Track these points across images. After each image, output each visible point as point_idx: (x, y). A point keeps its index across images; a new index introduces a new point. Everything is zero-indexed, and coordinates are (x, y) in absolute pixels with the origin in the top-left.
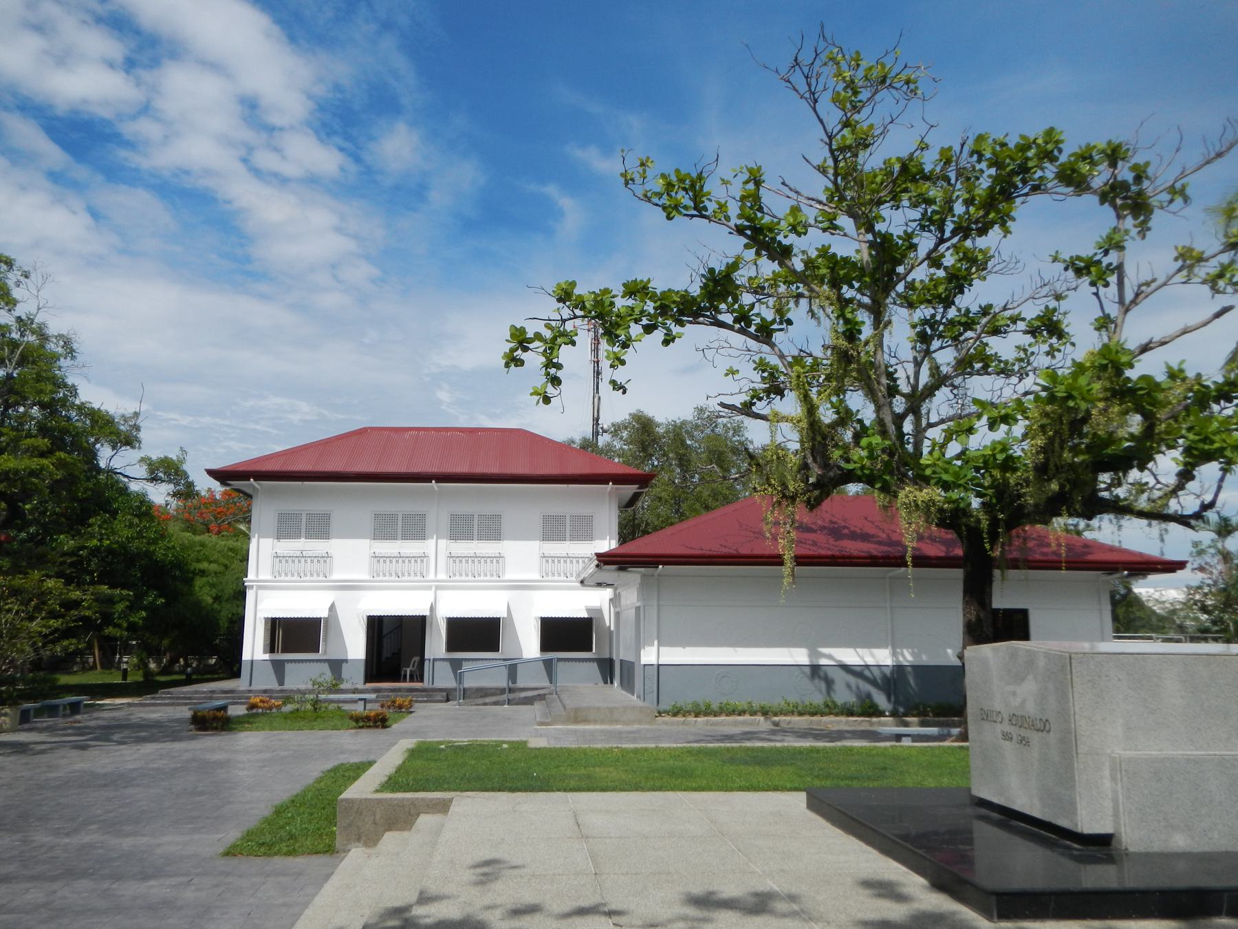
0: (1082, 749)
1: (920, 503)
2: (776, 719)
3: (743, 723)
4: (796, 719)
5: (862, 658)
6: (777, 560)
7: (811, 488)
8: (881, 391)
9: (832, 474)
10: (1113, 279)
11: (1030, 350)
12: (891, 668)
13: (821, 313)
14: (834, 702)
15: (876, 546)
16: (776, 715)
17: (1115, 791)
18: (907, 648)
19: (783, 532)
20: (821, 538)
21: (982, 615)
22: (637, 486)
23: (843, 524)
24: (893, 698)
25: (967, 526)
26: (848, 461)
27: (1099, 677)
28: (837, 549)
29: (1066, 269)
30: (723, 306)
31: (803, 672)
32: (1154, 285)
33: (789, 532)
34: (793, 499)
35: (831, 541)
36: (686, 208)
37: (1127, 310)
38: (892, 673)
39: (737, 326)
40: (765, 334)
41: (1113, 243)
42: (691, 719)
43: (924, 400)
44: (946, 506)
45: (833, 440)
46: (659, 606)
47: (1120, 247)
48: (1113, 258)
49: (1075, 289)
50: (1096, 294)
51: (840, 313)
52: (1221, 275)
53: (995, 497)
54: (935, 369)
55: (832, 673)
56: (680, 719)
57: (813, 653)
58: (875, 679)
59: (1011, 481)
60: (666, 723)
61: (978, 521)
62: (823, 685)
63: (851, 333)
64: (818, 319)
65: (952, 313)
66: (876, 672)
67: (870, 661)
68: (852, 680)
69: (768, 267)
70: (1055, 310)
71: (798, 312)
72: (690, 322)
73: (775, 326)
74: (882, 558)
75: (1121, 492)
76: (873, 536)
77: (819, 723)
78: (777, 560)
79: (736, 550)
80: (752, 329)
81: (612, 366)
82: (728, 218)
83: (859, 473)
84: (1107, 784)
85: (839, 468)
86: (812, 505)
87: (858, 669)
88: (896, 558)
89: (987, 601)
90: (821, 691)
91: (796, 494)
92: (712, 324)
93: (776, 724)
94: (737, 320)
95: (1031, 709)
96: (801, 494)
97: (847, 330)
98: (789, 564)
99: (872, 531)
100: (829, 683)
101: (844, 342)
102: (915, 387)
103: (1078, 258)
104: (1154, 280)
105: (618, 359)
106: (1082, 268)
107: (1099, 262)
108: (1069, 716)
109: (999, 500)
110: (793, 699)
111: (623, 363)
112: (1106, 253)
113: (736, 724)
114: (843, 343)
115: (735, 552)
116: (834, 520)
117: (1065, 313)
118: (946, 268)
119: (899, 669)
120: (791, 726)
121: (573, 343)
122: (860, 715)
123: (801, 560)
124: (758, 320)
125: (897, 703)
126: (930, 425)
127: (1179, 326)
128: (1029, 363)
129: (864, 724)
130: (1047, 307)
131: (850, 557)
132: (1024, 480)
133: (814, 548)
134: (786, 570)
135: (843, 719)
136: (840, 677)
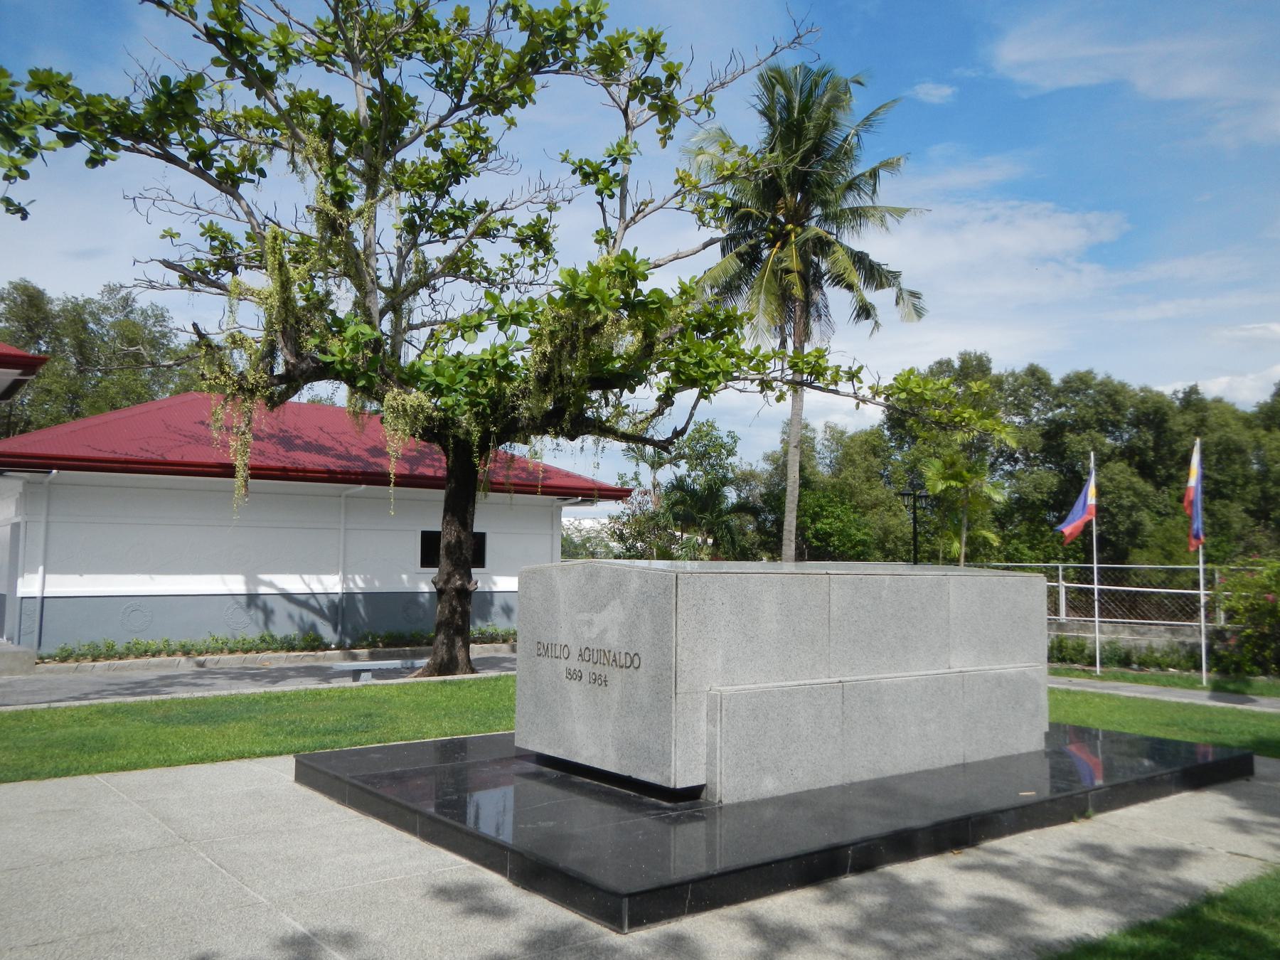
0: (682, 687)
1: (408, 407)
2: (201, 658)
3: (158, 666)
4: (226, 657)
5: (308, 586)
6: (227, 471)
7: (276, 381)
8: (369, 274)
9: (304, 366)
10: (617, 191)
12: (340, 595)
14: (272, 636)
15: (334, 460)
16: (200, 654)
17: (711, 736)
18: (359, 574)
19: (237, 433)
20: (269, 447)
21: (463, 537)
22: (19, 371)
23: (295, 433)
24: (339, 628)
25: (455, 437)
26: (324, 352)
27: (704, 600)
28: (287, 461)
29: (574, 172)
30: (175, 136)
31: (237, 603)
32: (651, 207)
33: (244, 433)
34: (252, 392)
35: (282, 451)
37: (627, 227)
38: (341, 600)
39: (193, 165)
40: (228, 182)
41: (620, 155)
42: (87, 664)
43: (407, 297)
44: (435, 413)
45: (308, 325)
46: (47, 522)
48: (619, 168)
49: (570, 201)
50: (601, 204)
51: (330, 171)
53: (490, 407)
55: (271, 603)
56: (71, 664)
57: (251, 579)
58: (321, 608)
59: (508, 391)
60: (51, 671)
61: (468, 433)
62: (260, 616)
63: (341, 201)
65: (444, 206)
66: (324, 602)
67: (317, 589)
68: (296, 610)
69: (240, 98)
70: (546, 221)
72: (127, 149)
74: (341, 473)
75: (605, 413)
76: (331, 449)
77: (254, 661)
78: (227, 471)
79: (162, 455)
80: (213, 173)
83: (338, 367)
84: (703, 726)
87: (303, 598)
88: (356, 474)
89: (469, 521)
90: (257, 623)
91: (257, 387)
92: (157, 156)
93: (201, 665)
94: (193, 157)
95: (613, 640)
96: (263, 387)
97: (336, 194)
98: (241, 473)
99: (329, 443)
100: (268, 613)
101: (332, 208)
102: (397, 282)
103: (588, 162)
106: (588, 173)
107: (607, 170)
108: (670, 649)
109: (494, 410)
110: (222, 634)
112: (614, 162)
113: (148, 667)
115: (159, 458)
116: (284, 428)
118: (444, 151)
119: (349, 596)
120: (219, 666)
122: (303, 650)
123: (257, 472)
124: (222, 164)
125: (344, 633)
126: (412, 327)
127: (672, 252)
128: (512, 276)
129: (307, 658)
130: (539, 216)
131: (305, 470)
132: (521, 391)
133: (262, 458)
134: (238, 481)
135: (283, 654)
136: (281, 607)
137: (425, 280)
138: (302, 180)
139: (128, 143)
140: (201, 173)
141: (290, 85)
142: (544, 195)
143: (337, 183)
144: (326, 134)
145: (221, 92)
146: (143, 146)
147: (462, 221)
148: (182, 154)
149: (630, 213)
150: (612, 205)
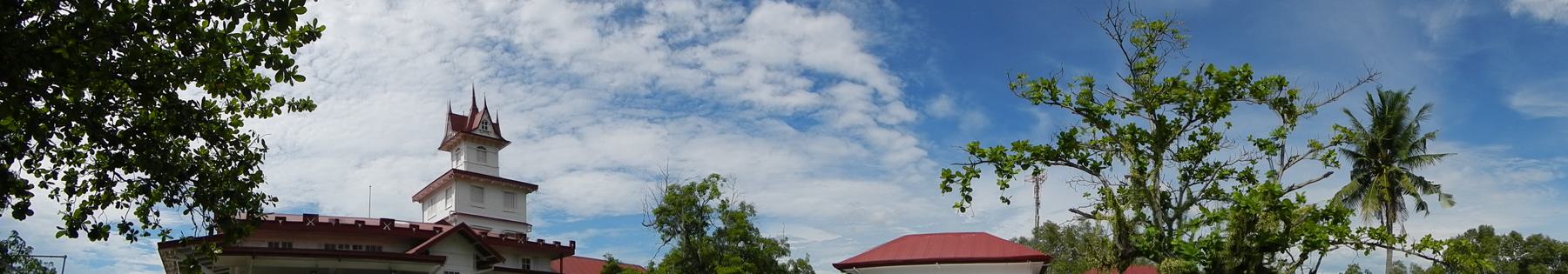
10: (1279, 152)
11: (1239, 189)
36: (1045, 98)
37: (1284, 169)
41: (1280, 134)
47: (1284, 136)
48: (1280, 142)
52: (1329, 156)
54: (1190, 194)
64: (1124, 162)
71: (1115, 160)
82: (1071, 105)
104: (1298, 156)
106: (1262, 145)
112: (1277, 138)
114: (1137, 175)
117: (1257, 172)
137: (1192, 201)
138: (1125, 164)
141: (1116, 125)
143: (1140, 163)
144: (1134, 142)
149: (1285, 163)
150: (1276, 159)
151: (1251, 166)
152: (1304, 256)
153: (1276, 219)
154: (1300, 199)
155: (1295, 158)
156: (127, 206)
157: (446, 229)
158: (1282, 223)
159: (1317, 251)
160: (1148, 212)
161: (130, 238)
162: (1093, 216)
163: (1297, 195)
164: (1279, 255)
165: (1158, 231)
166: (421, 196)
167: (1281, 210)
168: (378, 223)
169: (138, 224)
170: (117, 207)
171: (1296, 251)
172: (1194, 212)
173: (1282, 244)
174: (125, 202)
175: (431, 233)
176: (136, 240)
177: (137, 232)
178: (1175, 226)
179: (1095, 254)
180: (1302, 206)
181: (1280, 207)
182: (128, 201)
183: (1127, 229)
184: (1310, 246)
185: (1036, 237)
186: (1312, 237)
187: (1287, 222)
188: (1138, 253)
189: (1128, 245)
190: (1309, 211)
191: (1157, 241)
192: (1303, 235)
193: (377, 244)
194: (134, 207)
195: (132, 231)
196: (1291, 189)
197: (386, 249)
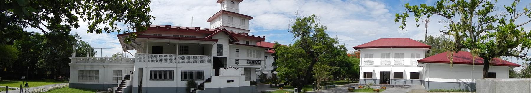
10: (514, 12)
13: (460, 13)
30: (441, 11)
37: (515, 19)
40: (449, 17)
48: (514, 8)
50: (511, 15)
72: (435, 14)
73: (452, 15)
80: (447, 16)
81: (416, 21)
85: (462, 44)
86: (457, 52)
92: (439, 14)
94: (444, 14)
103: (508, 7)
105: (418, 20)
106: (508, 9)
107: (512, 8)
111: (419, 21)
112: (513, 7)
117: (506, 20)
121: (409, 17)
124: (448, 14)
139: (435, 13)
140: (445, 16)
142: (503, 14)
145: (449, 2)
146: (437, 13)
147: (489, 19)
148: (442, 13)
151: (504, 17)
152: (522, 49)
153: (514, 36)
154: (522, 30)
155: (519, 14)
156: (106, 23)
157: (218, 30)
158: (515, 38)
159: (527, 48)
160: (468, 33)
161: (109, 32)
162: (447, 34)
163: (521, 28)
164: (514, 49)
165: (471, 40)
166: (210, 20)
167: (516, 33)
168: (194, 29)
169: (110, 28)
170: (104, 23)
171: (519, 48)
172: (483, 34)
173: (515, 45)
174: (106, 21)
175: (214, 32)
176: (110, 33)
177: (110, 31)
178: (476, 38)
179: (448, 46)
180: (522, 32)
181: (515, 32)
182: (107, 21)
183: (459, 38)
184: (525, 46)
185: (426, 40)
186: (526, 42)
187: (517, 37)
188: (464, 46)
189: (459, 44)
190: (524, 34)
191: (471, 43)
192: (522, 42)
193: (194, 36)
194: (109, 23)
195: (109, 30)
196: (518, 26)
197: (196, 37)
